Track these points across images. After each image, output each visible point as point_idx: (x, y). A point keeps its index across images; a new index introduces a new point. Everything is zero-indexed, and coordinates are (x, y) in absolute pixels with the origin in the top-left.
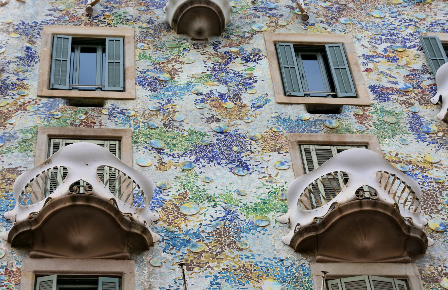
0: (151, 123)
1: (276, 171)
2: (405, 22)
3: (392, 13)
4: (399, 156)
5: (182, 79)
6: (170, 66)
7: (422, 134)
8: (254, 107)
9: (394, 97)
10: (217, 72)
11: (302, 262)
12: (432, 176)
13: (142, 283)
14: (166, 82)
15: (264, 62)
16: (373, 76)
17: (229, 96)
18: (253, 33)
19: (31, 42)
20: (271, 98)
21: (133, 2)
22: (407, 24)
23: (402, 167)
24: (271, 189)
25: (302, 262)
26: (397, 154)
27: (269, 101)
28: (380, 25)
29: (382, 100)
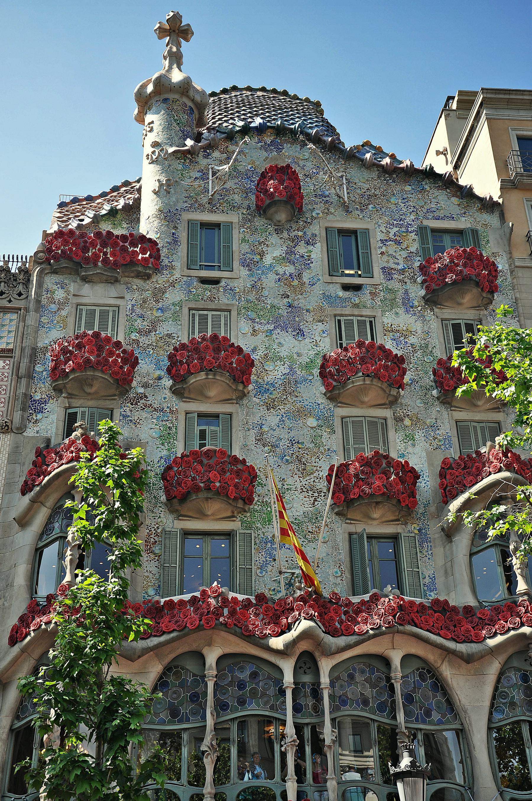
3: (403, 199)
5: (268, 260)
6: (260, 248)
9: (396, 276)
10: (288, 257)
11: (330, 406)
12: (410, 342)
13: (243, 420)
15: (318, 245)
19: (175, 228)
22: (411, 210)
25: (330, 406)
26: (391, 325)
27: (319, 280)
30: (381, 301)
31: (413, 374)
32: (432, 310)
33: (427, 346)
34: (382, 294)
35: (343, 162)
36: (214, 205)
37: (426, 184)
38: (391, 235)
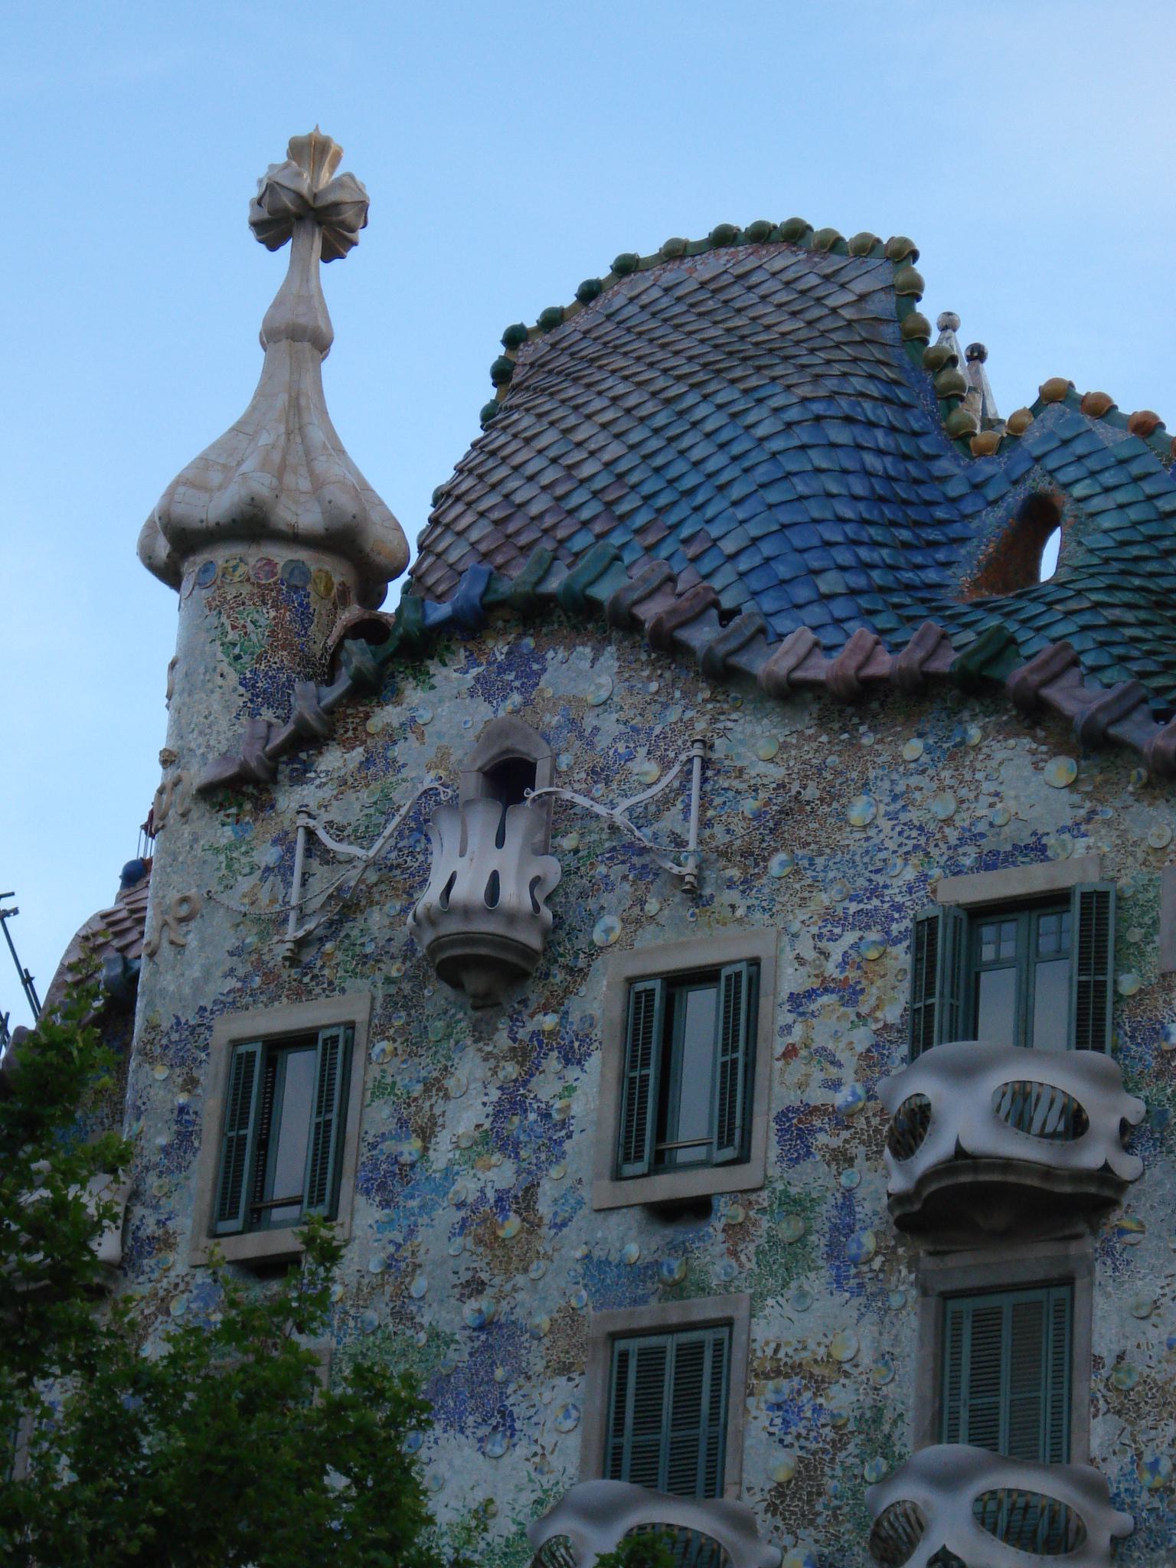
0: (371, 1316)
1: (555, 1437)
2: (908, 838)
3: (895, 798)
4: (781, 1354)
5: (442, 1153)
7: (843, 1265)
8: (555, 1225)
9: (822, 1139)
14: (413, 1166)
15: (594, 1062)
16: (797, 1069)
17: (516, 1197)
18: (595, 951)
19: (190, 1084)
20: (585, 1193)
21: (383, 887)
23: (777, 1391)
24: (539, 1494)
26: (776, 1351)
27: (580, 1203)
28: (857, 858)
29: (790, 1160)
30: (757, 1254)
31: (821, 1536)
32: (913, 1264)
33: (877, 1420)
34: (765, 1223)
35: (707, 694)
36: (309, 967)
37: (974, 717)
38: (831, 969)
